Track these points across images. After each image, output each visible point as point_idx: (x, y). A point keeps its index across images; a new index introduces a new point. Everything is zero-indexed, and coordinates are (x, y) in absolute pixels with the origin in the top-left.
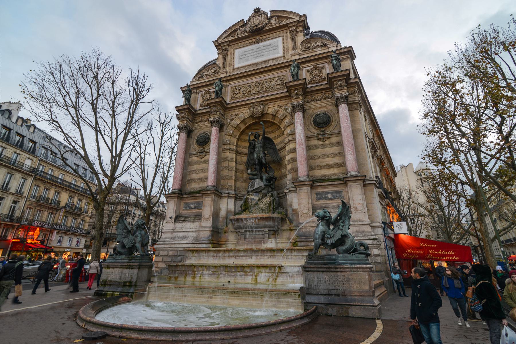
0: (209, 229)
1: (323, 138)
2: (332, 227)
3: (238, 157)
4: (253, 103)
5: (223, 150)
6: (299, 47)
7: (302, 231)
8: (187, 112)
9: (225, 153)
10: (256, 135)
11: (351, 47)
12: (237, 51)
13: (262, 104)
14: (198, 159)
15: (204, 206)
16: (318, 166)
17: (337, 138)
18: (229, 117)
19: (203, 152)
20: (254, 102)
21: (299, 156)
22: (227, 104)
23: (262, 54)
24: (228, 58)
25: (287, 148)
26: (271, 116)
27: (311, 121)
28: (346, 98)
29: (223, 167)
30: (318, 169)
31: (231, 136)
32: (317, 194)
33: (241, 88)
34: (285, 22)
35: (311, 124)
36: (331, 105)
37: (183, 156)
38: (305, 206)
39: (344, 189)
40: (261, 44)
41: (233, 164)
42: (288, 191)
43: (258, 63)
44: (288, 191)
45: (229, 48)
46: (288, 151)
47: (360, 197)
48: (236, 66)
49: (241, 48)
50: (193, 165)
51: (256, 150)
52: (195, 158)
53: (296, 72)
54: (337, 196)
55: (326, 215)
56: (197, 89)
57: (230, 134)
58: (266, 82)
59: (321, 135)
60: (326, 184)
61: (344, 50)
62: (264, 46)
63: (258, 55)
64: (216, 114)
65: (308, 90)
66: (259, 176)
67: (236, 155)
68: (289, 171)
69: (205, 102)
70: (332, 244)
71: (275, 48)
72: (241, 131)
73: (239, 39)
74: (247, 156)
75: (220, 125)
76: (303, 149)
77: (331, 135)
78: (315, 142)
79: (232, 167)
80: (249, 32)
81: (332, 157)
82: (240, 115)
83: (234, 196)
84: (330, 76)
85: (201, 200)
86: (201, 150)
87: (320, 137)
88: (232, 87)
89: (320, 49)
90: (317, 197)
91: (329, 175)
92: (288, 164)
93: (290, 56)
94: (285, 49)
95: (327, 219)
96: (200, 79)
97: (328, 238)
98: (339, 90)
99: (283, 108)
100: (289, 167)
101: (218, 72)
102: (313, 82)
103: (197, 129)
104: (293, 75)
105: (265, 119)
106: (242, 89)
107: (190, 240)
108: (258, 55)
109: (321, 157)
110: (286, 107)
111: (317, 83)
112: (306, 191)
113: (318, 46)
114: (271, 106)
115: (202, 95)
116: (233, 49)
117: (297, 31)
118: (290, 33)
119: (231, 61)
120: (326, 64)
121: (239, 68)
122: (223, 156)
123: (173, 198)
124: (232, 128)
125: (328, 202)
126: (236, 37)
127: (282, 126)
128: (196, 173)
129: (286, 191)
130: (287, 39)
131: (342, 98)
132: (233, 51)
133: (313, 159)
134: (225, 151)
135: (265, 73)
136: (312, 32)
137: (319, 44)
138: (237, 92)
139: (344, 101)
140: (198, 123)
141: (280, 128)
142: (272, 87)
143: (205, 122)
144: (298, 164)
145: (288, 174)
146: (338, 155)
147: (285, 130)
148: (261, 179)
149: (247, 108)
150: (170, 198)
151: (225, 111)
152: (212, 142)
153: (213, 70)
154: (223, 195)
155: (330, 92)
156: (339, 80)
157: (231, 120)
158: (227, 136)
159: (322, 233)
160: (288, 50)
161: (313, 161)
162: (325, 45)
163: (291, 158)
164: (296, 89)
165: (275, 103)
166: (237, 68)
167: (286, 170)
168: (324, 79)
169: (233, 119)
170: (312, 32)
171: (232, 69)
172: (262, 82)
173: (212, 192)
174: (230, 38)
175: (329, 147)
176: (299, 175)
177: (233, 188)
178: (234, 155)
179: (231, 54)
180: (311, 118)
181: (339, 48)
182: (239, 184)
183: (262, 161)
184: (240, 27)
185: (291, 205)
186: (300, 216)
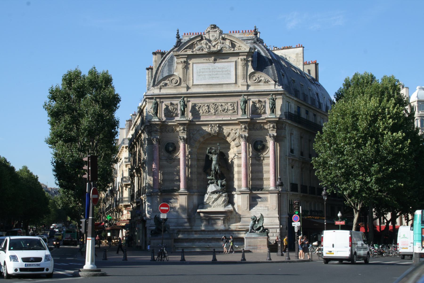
4: (211, 124)
23: (217, 76)
34: (237, 50)
40: (216, 64)
43: (214, 84)
47: (275, 202)
49: (198, 63)
51: (214, 162)
52: (165, 163)
54: (264, 200)
63: (214, 76)
68: (236, 179)
71: (229, 72)
73: (196, 54)
80: (207, 52)
93: (240, 84)
99: (233, 131)
108: (214, 76)
110: (236, 132)
113: (261, 80)
126: (195, 53)
146: (267, 172)
162: (267, 82)
166: (196, 85)
174: (189, 52)
184: (197, 41)
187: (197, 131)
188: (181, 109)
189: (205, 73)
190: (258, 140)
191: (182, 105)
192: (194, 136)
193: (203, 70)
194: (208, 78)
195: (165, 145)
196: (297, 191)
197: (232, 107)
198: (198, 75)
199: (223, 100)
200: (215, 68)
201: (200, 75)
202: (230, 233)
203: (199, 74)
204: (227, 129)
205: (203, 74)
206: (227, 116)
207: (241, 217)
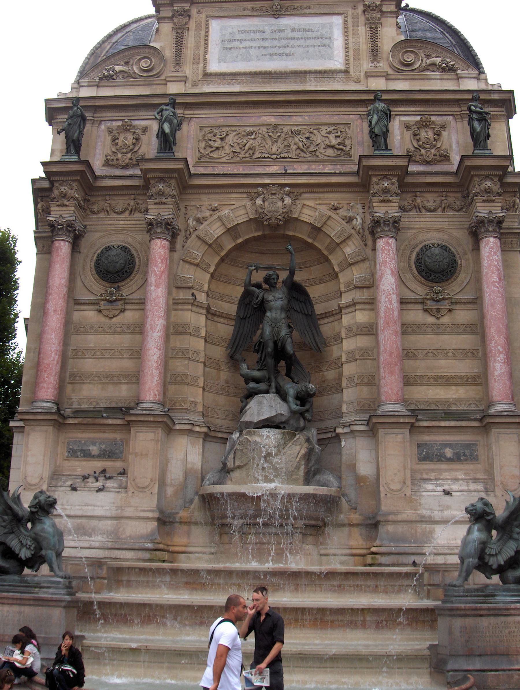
0: (150, 515)
1: (438, 310)
2: (494, 533)
3: (209, 322)
4: (264, 186)
5: (173, 303)
6: (385, 56)
7: (387, 532)
8: (74, 181)
9: (180, 312)
10: (270, 276)
11: (511, 92)
12: (215, 25)
13: (288, 194)
14: (103, 319)
15: (136, 454)
16: (421, 377)
17: (469, 312)
18: (193, 213)
19: (116, 300)
20: (268, 184)
21: (386, 349)
22: (191, 175)
23: (287, 50)
25: (346, 320)
26: (307, 229)
27: (409, 260)
28: (500, 222)
29: (173, 349)
30: (421, 385)
31: (197, 265)
32: (419, 446)
33: (227, 135)
35: (410, 267)
36: (460, 228)
37: (64, 308)
38: (395, 474)
39: (479, 438)
40: (286, 22)
41: (201, 344)
42: (346, 430)
43: (276, 73)
44: (346, 430)
45: (194, 11)
46: (349, 329)
48: (214, 67)
50: (86, 333)
53: (384, 129)
54: (464, 454)
55: (488, 510)
56: (95, 112)
57: (197, 261)
58: (299, 133)
59: (434, 300)
60: (443, 424)
61: (496, 96)
62: (293, 30)
63: (276, 51)
64: (165, 203)
65: (409, 180)
66: (273, 385)
67: (207, 318)
68: (350, 379)
69: (120, 156)
70: (500, 566)
71: (326, 42)
72: (223, 254)
74: (233, 323)
75: (173, 233)
76: (396, 333)
77: (456, 303)
79: (197, 352)
81: (455, 358)
82: (225, 211)
83: (205, 429)
84: (468, 163)
85: (118, 436)
86: (111, 294)
87: (430, 304)
88: (202, 127)
89: (437, 74)
90: (420, 454)
91: (447, 402)
92: (348, 362)
93: (362, 74)
94: (351, 53)
95: (489, 518)
96: (104, 83)
97: (491, 555)
98: (484, 201)
99: (342, 212)
100: (348, 369)
101: (158, 75)
102: (417, 158)
103: (96, 231)
104: (373, 136)
105: (290, 233)
106: (231, 139)
107: (97, 540)
108: (276, 51)
109: (431, 355)
110: (351, 214)
111: (428, 163)
112: (400, 438)
113: (433, 64)
114: (311, 203)
115: (110, 131)
116: (203, 16)
117: (381, 11)
118: (364, 11)
119: (197, 47)
120: (451, 117)
121: (221, 76)
122: (173, 319)
123: (43, 423)
124: (199, 243)
125: (444, 466)
127: (335, 260)
128: (94, 357)
129: (339, 430)
130: (356, 25)
131: (490, 221)
132: (203, 21)
133: (408, 359)
134: (180, 307)
135: (297, 107)
136: (407, 5)
137: (438, 60)
138: (216, 145)
139: (494, 231)
140: (99, 212)
141: (327, 260)
142: (312, 148)
143: (122, 213)
144: (382, 371)
145: (347, 388)
146: (469, 354)
147: (342, 270)
148: (283, 395)
149: (245, 196)
150: (32, 423)
151: (181, 193)
152: (152, 279)
153: (144, 64)
154: (178, 427)
155: (459, 195)
156: (487, 177)
157: (199, 221)
158: (187, 266)
159: (482, 545)
161: (411, 362)
162: (451, 69)
163: (360, 349)
164: (385, 177)
165: (321, 195)
167: (340, 375)
168: (445, 156)
169: (205, 219)
170: (407, 5)
171: (201, 72)
172: (286, 129)
173: (160, 419)
175: (449, 334)
176: (383, 398)
177: (200, 408)
178: (202, 319)
180: (412, 252)
181: (483, 86)
182: (210, 397)
183: (283, 348)
185: (353, 467)
186: (382, 495)
187: (214, 210)
188: (163, 132)
189: (247, 42)
191: (165, 120)
192: (202, 227)
193: (242, 35)
194: (257, 57)
195: (96, 255)
197: (336, 137)
198: (226, 48)
199: (307, 118)
200: (280, 31)
201: (230, 48)
202: (340, 586)
203: (228, 46)
204: (318, 206)
205: (241, 46)
206: (321, 167)
207: (379, 518)
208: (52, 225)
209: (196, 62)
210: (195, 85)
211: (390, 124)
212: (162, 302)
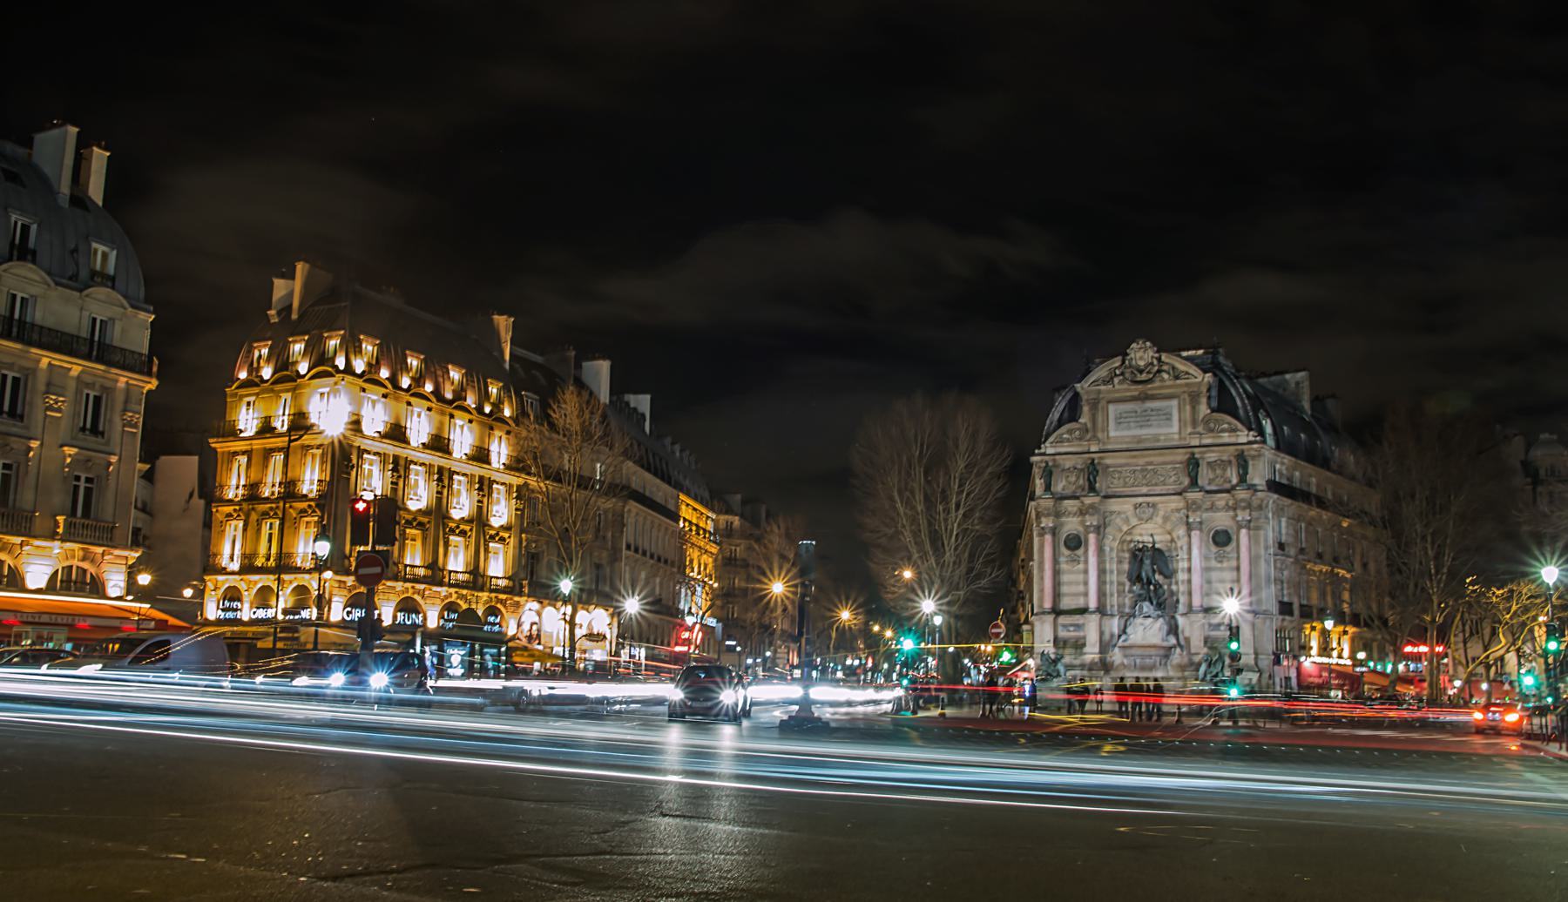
12: (1111, 407)
24: (1100, 419)
78: (1214, 563)
89: (1226, 434)
100: (1182, 588)
119: (1103, 421)
130: (1184, 405)
160: (1185, 426)
179: (1103, 408)
185: (1183, 632)
190: (1218, 528)
196: (1291, 613)
208: (1043, 528)
209: (1103, 431)
210: (1104, 443)
211: (1200, 469)
212: (1095, 564)
